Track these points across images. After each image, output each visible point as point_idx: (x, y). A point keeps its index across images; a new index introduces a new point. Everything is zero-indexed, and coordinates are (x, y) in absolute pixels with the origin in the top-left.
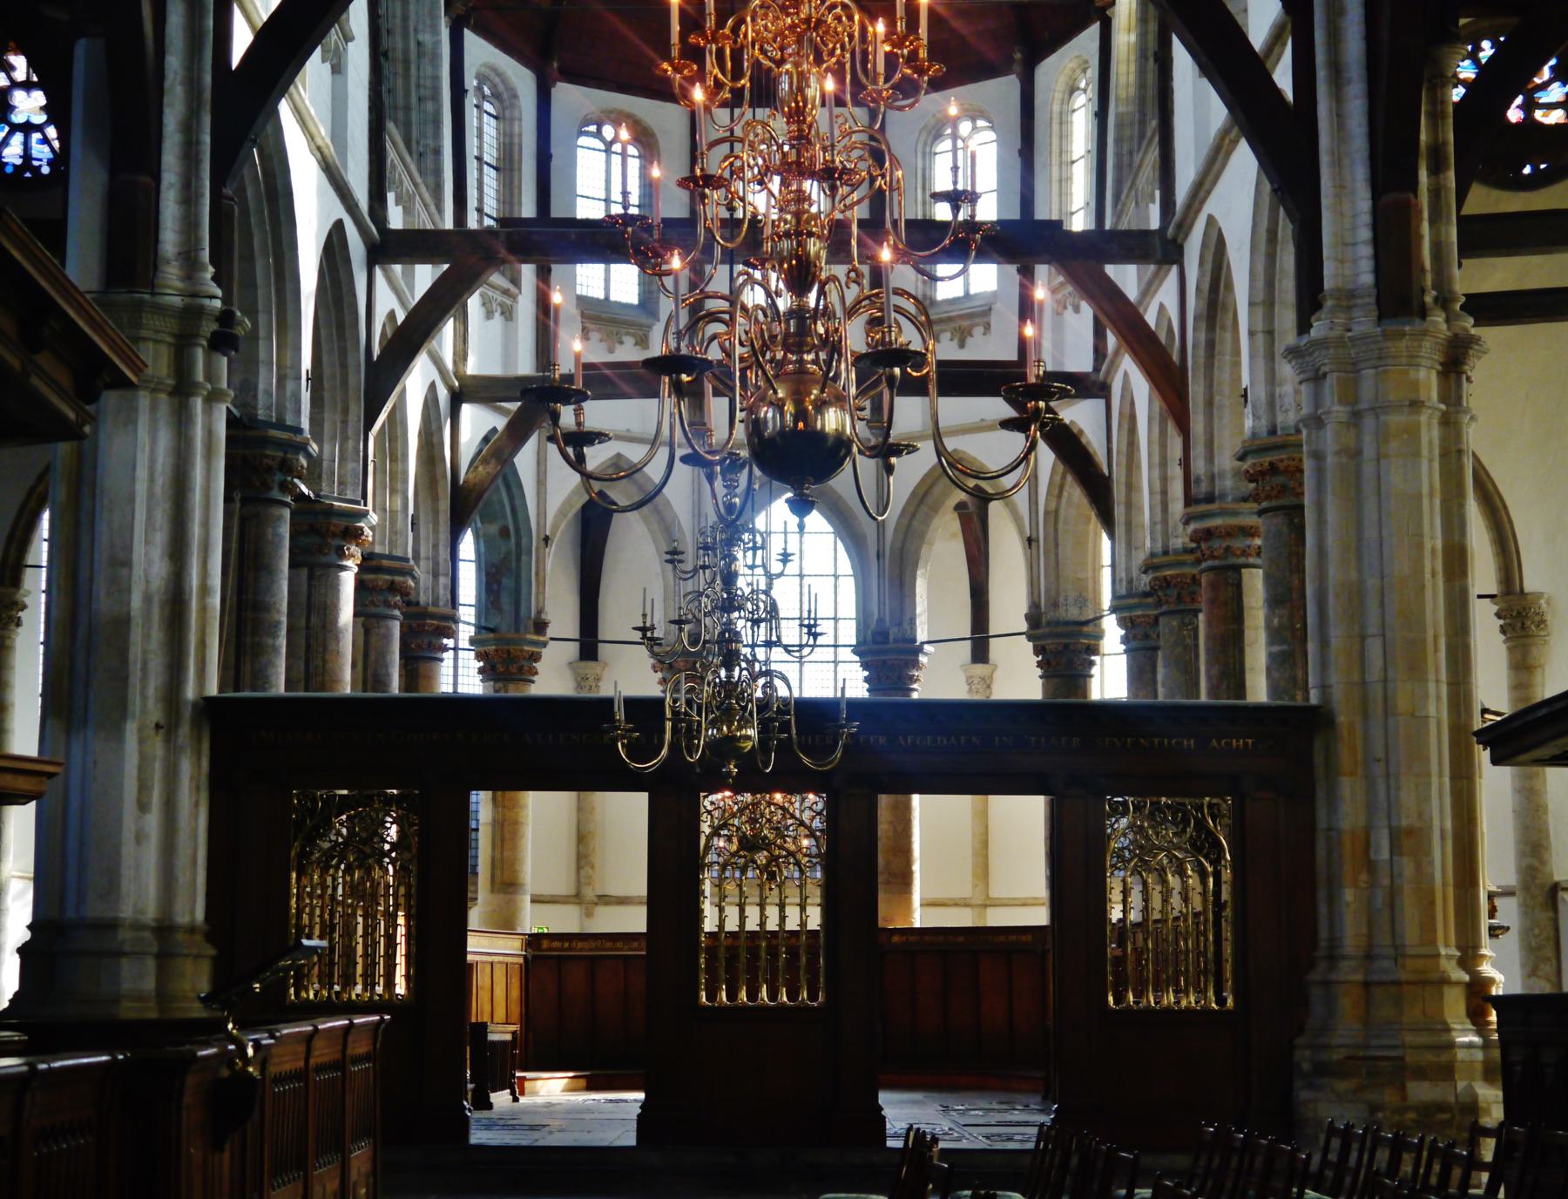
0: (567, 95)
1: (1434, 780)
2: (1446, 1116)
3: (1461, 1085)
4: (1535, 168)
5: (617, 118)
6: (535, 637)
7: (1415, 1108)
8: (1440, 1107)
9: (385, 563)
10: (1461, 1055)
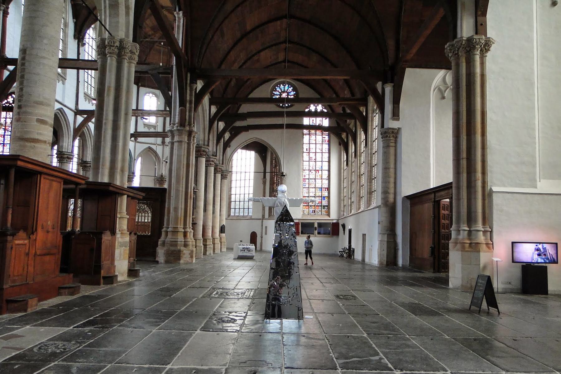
0: (142, 89)
1: (180, 200)
2: (175, 252)
3: (179, 248)
4: (288, 105)
5: (153, 93)
6: (132, 175)
7: (171, 251)
8: (175, 251)
9: (89, 162)
10: (179, 243)
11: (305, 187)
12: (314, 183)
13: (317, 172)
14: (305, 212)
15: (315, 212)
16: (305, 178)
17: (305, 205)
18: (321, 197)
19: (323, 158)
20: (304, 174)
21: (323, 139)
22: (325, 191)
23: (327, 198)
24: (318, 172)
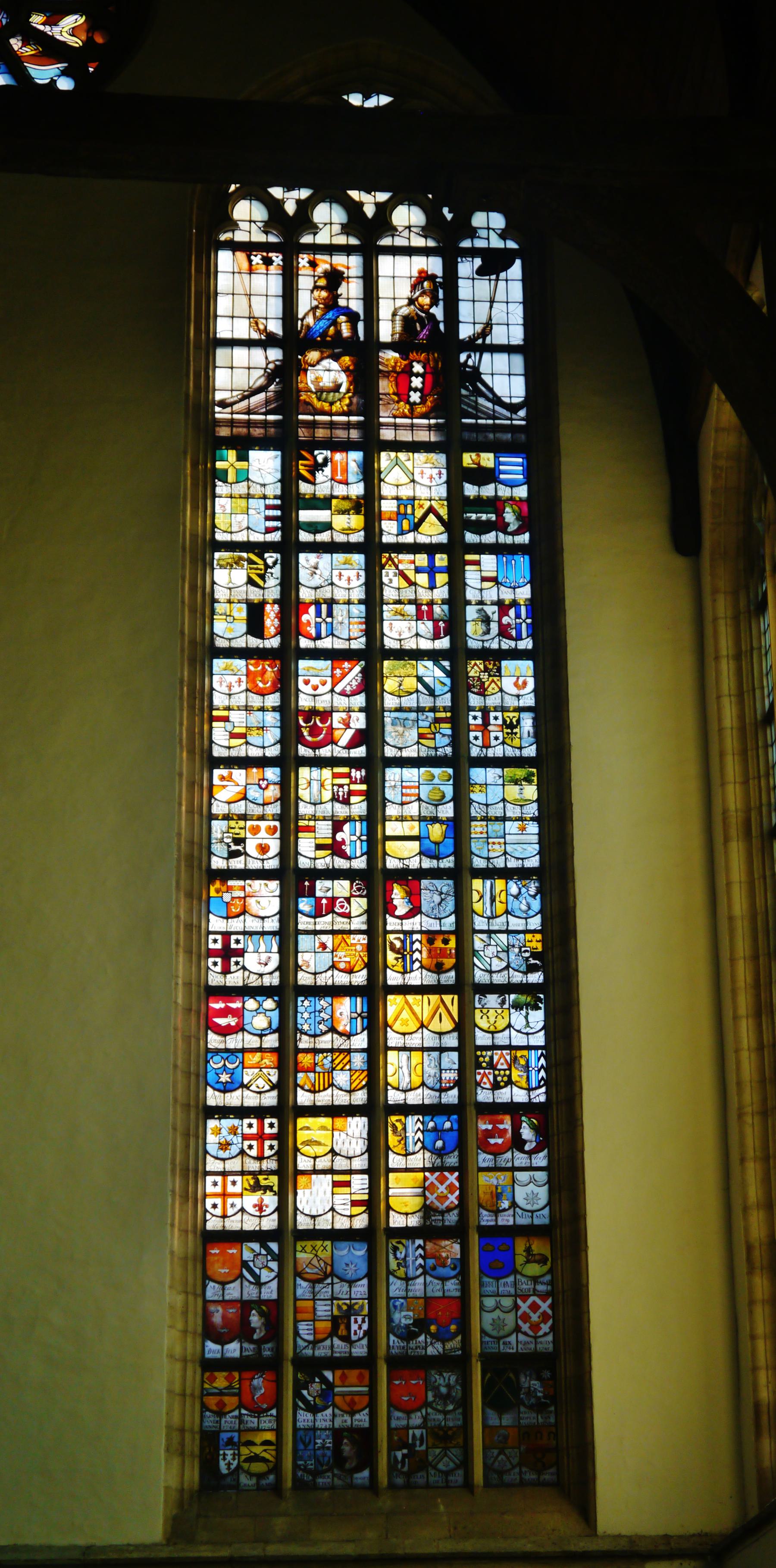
11: (233, 1099)
12: (361, 1041)
13: (398, 895)
14: (227, 1461)
15: (367, 1458)
16: (235, 979)
17: (233, 1349)
18: (459, 1232)
19: (475, 719)
20: (216, 924)
21: (470, 490)
22: (521, 1159)
23: (539, 1247)
24: (414, 897)
